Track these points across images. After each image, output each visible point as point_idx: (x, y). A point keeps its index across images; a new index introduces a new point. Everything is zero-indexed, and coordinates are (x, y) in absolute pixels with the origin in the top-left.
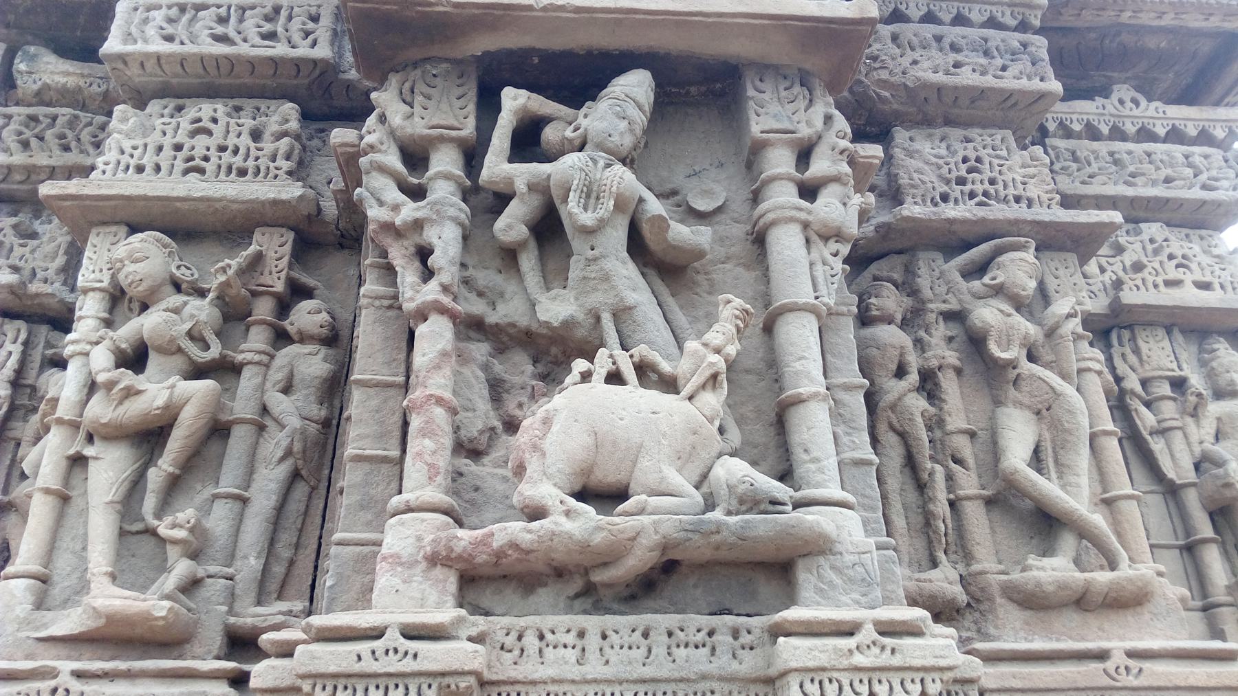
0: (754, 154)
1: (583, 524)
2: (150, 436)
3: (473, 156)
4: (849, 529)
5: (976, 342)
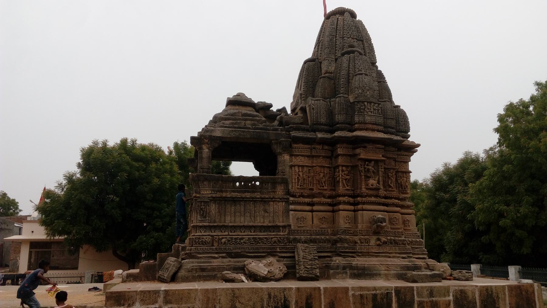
0: (379, 166)
1: (371, 187)
2: (346, 179)
3: (364, 165)
4: (382, 187)
5: (388, 175)
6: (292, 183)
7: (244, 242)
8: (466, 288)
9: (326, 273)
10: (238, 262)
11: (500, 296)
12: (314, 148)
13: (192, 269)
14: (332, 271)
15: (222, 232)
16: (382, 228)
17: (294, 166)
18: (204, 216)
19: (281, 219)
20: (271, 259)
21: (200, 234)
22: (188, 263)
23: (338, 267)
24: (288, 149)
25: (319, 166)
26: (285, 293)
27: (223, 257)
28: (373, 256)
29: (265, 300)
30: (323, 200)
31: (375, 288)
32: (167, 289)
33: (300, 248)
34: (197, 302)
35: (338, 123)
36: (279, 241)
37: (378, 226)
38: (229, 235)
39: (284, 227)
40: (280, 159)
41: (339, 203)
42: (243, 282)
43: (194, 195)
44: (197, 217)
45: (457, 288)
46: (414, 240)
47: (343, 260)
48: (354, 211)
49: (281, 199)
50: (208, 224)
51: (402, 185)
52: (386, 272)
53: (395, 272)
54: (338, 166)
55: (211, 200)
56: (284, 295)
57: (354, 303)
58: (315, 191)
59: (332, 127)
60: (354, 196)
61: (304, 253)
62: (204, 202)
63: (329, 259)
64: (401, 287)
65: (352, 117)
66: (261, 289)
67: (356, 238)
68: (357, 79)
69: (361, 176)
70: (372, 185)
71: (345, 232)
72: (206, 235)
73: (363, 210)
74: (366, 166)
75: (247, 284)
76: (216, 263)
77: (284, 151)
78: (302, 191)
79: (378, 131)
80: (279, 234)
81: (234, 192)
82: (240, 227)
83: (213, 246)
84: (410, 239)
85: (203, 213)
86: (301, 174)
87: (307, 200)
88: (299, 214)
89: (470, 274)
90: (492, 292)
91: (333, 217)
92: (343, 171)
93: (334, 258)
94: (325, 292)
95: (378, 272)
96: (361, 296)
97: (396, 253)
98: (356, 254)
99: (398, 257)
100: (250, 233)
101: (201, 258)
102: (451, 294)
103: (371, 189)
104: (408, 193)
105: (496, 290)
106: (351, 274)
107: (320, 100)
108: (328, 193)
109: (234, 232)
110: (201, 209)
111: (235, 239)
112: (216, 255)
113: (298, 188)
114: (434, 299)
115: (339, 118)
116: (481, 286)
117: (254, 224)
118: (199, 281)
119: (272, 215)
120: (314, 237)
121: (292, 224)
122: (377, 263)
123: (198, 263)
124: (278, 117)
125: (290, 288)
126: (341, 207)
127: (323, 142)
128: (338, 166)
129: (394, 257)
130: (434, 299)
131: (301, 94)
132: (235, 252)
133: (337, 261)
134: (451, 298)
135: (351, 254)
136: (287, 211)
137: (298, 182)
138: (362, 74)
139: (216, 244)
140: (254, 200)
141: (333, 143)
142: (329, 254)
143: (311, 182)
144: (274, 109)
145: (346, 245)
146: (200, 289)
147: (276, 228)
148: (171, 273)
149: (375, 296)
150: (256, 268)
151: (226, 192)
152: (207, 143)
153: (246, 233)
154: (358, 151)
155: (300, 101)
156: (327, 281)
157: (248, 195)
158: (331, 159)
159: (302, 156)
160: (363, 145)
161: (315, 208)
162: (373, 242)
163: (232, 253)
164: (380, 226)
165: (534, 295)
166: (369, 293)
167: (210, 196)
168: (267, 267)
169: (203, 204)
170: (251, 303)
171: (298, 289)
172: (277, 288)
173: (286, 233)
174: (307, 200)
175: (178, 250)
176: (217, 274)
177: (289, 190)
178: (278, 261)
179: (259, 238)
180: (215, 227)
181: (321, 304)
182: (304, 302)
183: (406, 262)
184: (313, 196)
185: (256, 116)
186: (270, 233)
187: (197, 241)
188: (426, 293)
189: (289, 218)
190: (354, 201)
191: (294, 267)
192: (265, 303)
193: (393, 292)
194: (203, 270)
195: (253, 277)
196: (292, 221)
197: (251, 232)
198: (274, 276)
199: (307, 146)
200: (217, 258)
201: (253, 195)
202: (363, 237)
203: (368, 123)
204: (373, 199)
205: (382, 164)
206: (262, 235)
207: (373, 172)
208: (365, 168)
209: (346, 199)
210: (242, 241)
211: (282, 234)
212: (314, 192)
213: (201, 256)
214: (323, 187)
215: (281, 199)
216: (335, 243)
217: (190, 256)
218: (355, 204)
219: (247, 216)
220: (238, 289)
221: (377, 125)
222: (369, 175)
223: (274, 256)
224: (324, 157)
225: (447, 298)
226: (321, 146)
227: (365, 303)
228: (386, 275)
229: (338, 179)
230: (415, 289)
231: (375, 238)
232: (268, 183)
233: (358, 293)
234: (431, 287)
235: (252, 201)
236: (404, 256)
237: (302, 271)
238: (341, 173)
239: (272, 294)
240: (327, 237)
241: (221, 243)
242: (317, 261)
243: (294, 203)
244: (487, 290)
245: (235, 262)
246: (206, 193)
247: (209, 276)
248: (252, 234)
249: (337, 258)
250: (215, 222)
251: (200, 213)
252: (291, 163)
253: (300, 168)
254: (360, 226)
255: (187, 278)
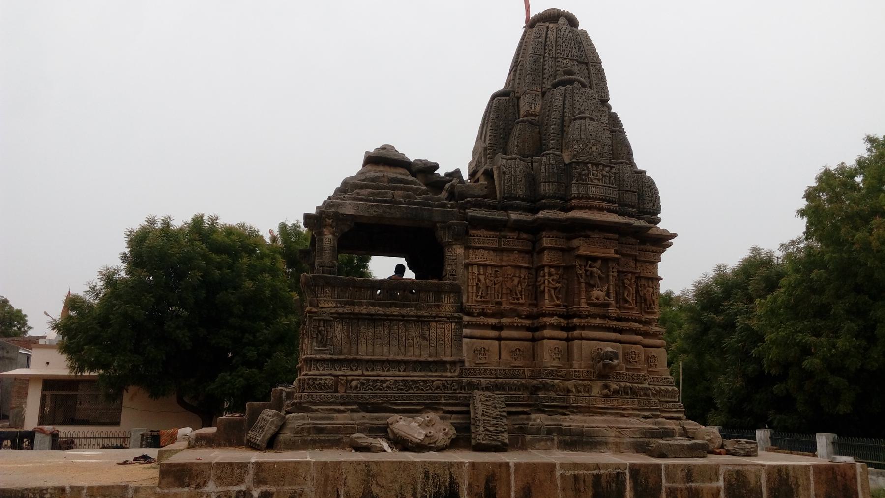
0: (609, 268)
2: (555, 288)
3: (585, 267)
4: (613, 302)
5: (624, 283)
6: (468, 292)
7: (388, 387)
8: (746, 468)
9: (518, 440)
10: (377, 419)
11: (800, 482)
12: (505, 237)
13: (303, 429)
14: (528, 437)
15: (351, 369)
16: (613, 367)
17: (472, 265)
18: (323, 342)
19: (448, 351)
20: (431, 415)
21: (317, 372)
22: (296, 419)
23: (538, 431)
24: (462, 237)
25: (511, 266)
26: (452, 471)
27: (352, 411)
28: (595, 413)
29: (419, 481)
30: (518, 321)
31: (598, 464)
32: (259, 460)
33: (478, 398)
34: (309, 483)
35: (544, 197)
36: (444, 386)
37: (605, 365)
38: (363, 375)
39: (453, 363)
40: (449, 253)
41: (544, 327)
42: (385, 451)
43: (308, 308)
44: (311, 344)
45: (730, 468)
46: (663, 388)
47: (547, 420)
48: (568, 340)
49: (448, 318)
50: (329, 356)
51: (645, 300)
52: (617, 439)
53: (632, 440)
54: (543, 267)
55: (335, 318)
56: (451, 475)
57: (564, 489)
58: (505, 306)
59: (534, 203)
60: (568, 316)
61: (484, 406)
62: (324, 320)
63: (524, 417)
64: (641, 465)
65: (568, 187)
66: (414, 463)
67: (569, 384)
68: (577, 126)
69: (580, 283)
70: (597, 299)
71: (552, 373)
72: (325, 374)
73: (582, 339)
74: (588, 268)
75: (391, 455)
76: (341, 419)
77: (456, 240)
78: (484, 306)
79: (609, 211)
80: (444, 374)
81: (373, 305)
82: (383, 362)
83: (337, 392)
84: (657, 387)
85: (322, 339)
86: (482, 278)
87: (491, 321)
88: (479, 343)
89: (753, 446)
90: (787, 475)
91: (534, 350)
92: (550, 275)
93: (533, 416)
94: (516, 470)
95: (603, 439)
96: (576, 477)
97: (633, 409)
98: (568, 409)
99: (638, 416)
100: (397, 373)
101: (317, 411)
102: (721, 478)
103: (595, 305)
104: (654, 313)
105: (794, 472)
106: (560, 442)
107: (515, 159)
108: (525, 310)
109: (372, 370)
110: (319, 332)
111: (375, 381)
112: (342, 408)
113: (476, 301)
114: (693, 485)
115: (546, 188)
116: (769, 466)
117: (406, 359)
118: (313, 449)
119: (433, 343)
120: (501, 380)
121: (466, 360)
122: (602, 425)
123: (312, 419)
124: (447, 185)
125: (461, 462)
126: (547, 333)
127: (518, 227)
128: (543, 267)
129: (630, 416)
130: (693, 485)
131: (485, 149)
132: (372, 404)
133: (539, 421)
134: (721, 483)
135: (560, 410)
136: (458, 338)
137: (478, 292)
138: (584, 118)
139: (341, 389)
140: (405, 319)
141: (535, 229)
142: (525, 409)
143: (498, 292)
144: (441, 172)
145: (553, 395)
146: (315, 462)
147: (441, 365)
148: (268, 436)
149: (598, 478)
150: (405, 429)
151: (361, 304)
152: (331, 226)
153: (390, 373)
154: (575, 243)
155: (483, 160)
156: (520, 452)
157: (395, 311)
158: (532, 256)
159: (485, 249)
160: (583, 234)
161: (505, 333)
162: (596, 391)
163: (368, 404)
164: (609, 364)
165: (856, 482)
166: (588, 473)
167: (333, 310)
168: (424, 428)
169: (322, 323)
170: (396, 486)
171: (473, 465)
172: (439, 463)
173: (456, 374)
174: (491, 321)
175: (281, 397)
176: (342, 438)
177: (462, 303)
178: (442, 418)
179: (412, 381)
180: (340, 361)
181: (510, 488)
182: (483, 486)
183: (650, 423)
184: (501, 314)
185: (412, 183)
186: (430, 374)
187: (311, 383)
188: (680, 475)
189: (461, 350)
190: (568, 324)
191: (467, 429)
192: (419, 487)
193: (627, 472)
194: (320, 430)
195: (402, 444)
196: (466, 355)
197: (399, 371)
198: (434, 443)
199: (492, 233)
200: (343, 412)
201: (404, 311)
202: (580, 382)
203: (593, 198)
204: (598, 321)
205: (615, 265)
206: (417, 376)
207: (600, 278)
208: (586, 271)
209: (554, 320)
210: (384, 385)
211: (449, 374)
212: (503, 308)
213: (317, 407)
214: (518, 299)
215: (448, 318)
216: (536, 391)
217: (299, 408)
218: (568, 329)
219: (393, 345)
220: (376, 463)
221: (608, 201)
222: (592, 282)
223: (436, 410)
224: (520, 251)
225: (715, 485)
226: (516, 234)
227: (582, 489)
228: (617, 445)
229: (542, 288)
230: (663, 467)
231: (600, 383)
232: (429, 291)
233: (569, 473)
234: (689, 465)
235: (401, 320)
236: (646, 414)
237: (480, 435)
238: (547, 277)
239: (431, 472)
240: (523, 381)
241: (351, 387)
242: (505, 420)
243: (470, 325)
244: (779, 471)
245: (372, 419)
246: (327, 305)
247: (329, 440)
248: (402, 374)
249: (537, 415)
250: (341, 354)
251: (317, 338)
252: (466, 261)
253: (482, 269)
254: (576, 364)
255: (294, 443)
